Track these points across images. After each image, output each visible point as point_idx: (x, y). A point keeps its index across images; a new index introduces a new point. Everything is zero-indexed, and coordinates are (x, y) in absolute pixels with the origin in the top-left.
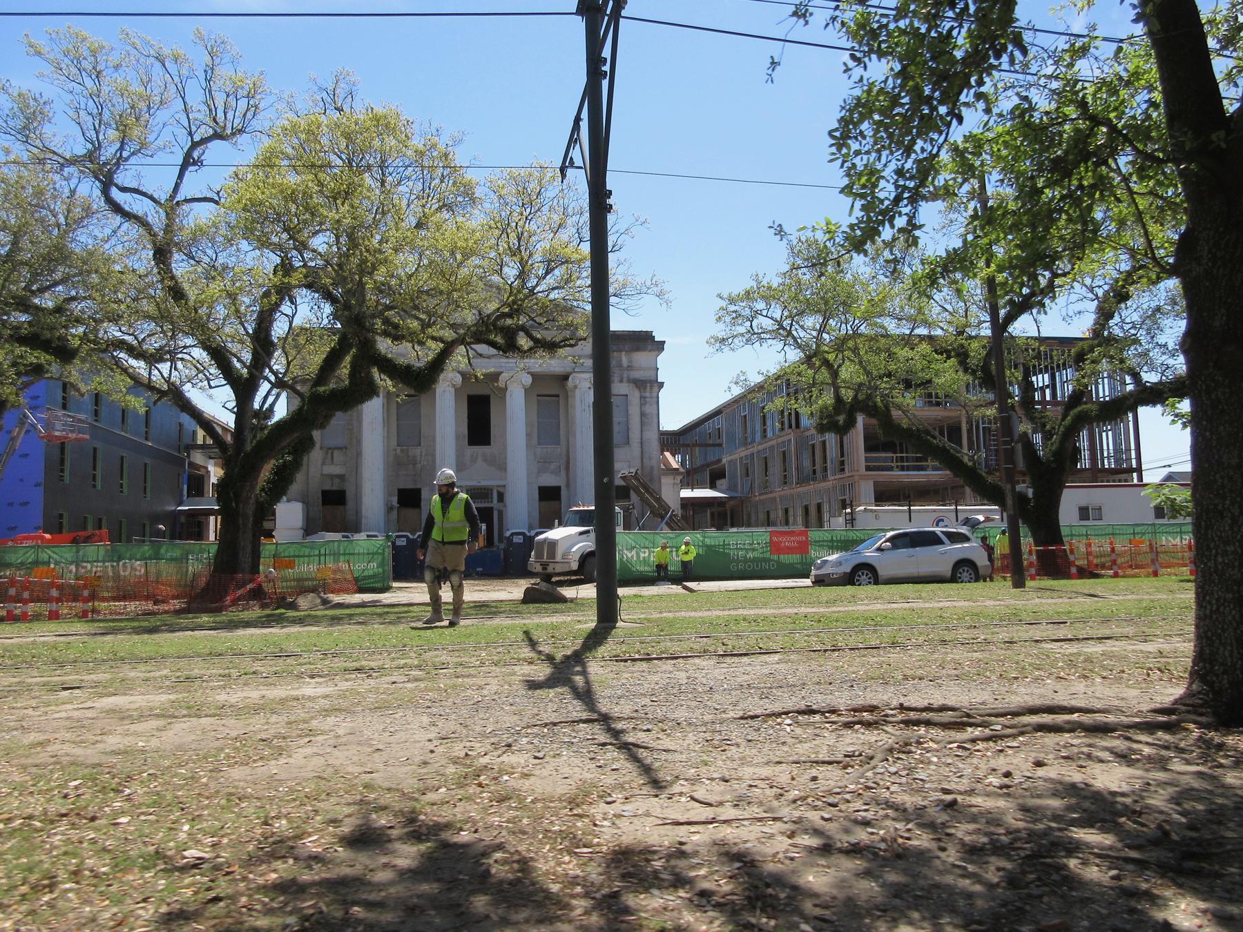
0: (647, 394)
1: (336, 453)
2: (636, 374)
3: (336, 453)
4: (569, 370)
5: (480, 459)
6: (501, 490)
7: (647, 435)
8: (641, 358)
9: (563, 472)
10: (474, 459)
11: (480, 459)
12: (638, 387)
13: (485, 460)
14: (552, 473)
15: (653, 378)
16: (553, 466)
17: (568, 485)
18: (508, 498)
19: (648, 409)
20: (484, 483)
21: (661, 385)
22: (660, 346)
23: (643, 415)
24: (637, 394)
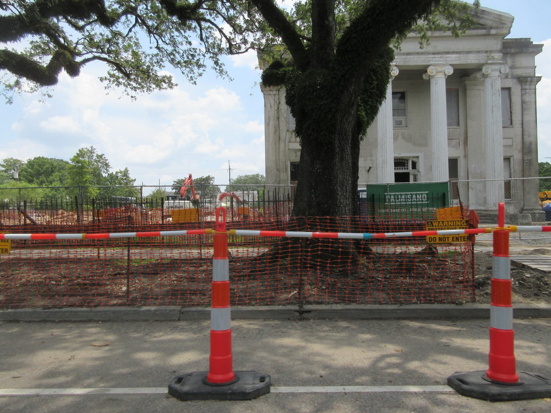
0: (527, 87)
2: (519, 72)
4: (482, 62)
5: (400, 137)
6: (415, 160)
7: (526, 118)
8: (522, 60)
9: (462, 147)
11: (400, 137)
13: (404, 138)
15: (532, 75)
16: (454, 142)
17: (466, 156)
18: (421, 166)
19: (527, 98)
20: (403, 155)
21: (539, 79)
22: (539, 48)
23: (523, 102)
24: (519, 87)
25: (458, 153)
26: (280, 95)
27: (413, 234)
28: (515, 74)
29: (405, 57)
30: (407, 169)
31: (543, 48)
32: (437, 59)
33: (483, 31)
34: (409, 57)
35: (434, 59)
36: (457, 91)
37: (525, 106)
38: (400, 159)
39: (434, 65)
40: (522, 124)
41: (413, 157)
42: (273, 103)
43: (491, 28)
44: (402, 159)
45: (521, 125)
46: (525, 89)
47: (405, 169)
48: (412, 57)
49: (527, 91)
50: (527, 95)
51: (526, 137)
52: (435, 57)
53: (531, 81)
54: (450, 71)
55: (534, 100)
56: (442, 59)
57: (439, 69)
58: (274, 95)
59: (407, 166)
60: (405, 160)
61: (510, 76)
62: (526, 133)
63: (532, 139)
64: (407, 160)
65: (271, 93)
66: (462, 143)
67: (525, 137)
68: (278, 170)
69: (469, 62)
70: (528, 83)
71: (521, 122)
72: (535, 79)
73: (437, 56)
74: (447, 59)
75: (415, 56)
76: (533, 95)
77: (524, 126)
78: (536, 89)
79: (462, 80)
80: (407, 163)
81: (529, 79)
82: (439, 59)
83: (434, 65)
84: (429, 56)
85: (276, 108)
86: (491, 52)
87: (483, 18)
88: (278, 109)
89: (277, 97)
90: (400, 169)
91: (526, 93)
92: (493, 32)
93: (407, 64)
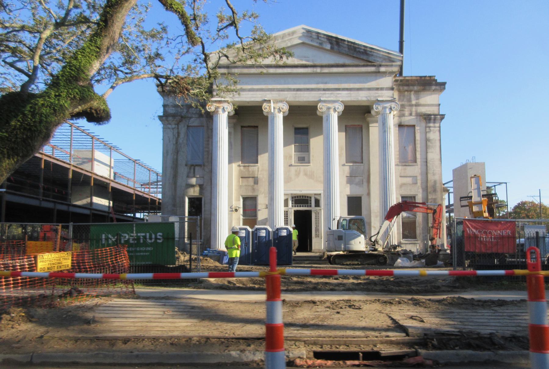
0: (431, 125)
1: (197, 168)
3: (197, 168)
6: (317, 197)
7: (430, 156)
9: (365, 184)
10: (298, 174)
12: (425, 119)
13: (306, 174)
14: (356, 184)
15: (436, 112)
16: (357, 180)
21: (442, 117)
22: (442, 86)
24: (423, 124)
25: (358, 192)
26: (180, 128)
27: (154, 277)
28: (419, 111)
29: (295, 92)
30: (310, 206)
31: (446, 86)
32: (327, 95)
33: (373, 69)
34: (299, 92)
35: (324, 96)
36: (361, 128)
37: (429, 143)
38: (303, 196)
39: (325, 101)
40: (427, 162)
41: (315, 194)
43: (380, 66)
44: (305, 197)
45: (425, 164)
46: (430, 127)
47: (308, 206)
48: (302, 93)
49: (432, 129)
50: (432, 132)
51: (430, 177)
52: (325, 94)
53: (435, 119)
54: (341, 108)
55: (438, 138)
56: (332, 95)
57: (329, 105)
58: (173, 129)
59: (311, 203)
60: (308, 197)
61: (414, 114)
62: (430, 172)
63: (437, 177)
64: (310, 198)
65: (170, 126)
66: (365, 180)
67: (429, 176)
68: (174, 205)
69: (360, 99)
70: (432, 121)
71: (425, 160)
72: (439, 117)
73: (327, 92)
74: (338, 96)
75: (306, 92)
76: (438, 133)
77: (428, 165)
78: (440, 127)
79: (357, 117)
80: (310, 201)
81: (432, 117)
82: (329, 95)
83: (325, 101)
84: (319, 92)
85: (175, 142)
86: (382, 89)
87: (372, 55)
88: (177, 143)
89: (176, 131)
90: (300, 206)
91: (429, 132)
92: (382, 69)
93: (297, 100)
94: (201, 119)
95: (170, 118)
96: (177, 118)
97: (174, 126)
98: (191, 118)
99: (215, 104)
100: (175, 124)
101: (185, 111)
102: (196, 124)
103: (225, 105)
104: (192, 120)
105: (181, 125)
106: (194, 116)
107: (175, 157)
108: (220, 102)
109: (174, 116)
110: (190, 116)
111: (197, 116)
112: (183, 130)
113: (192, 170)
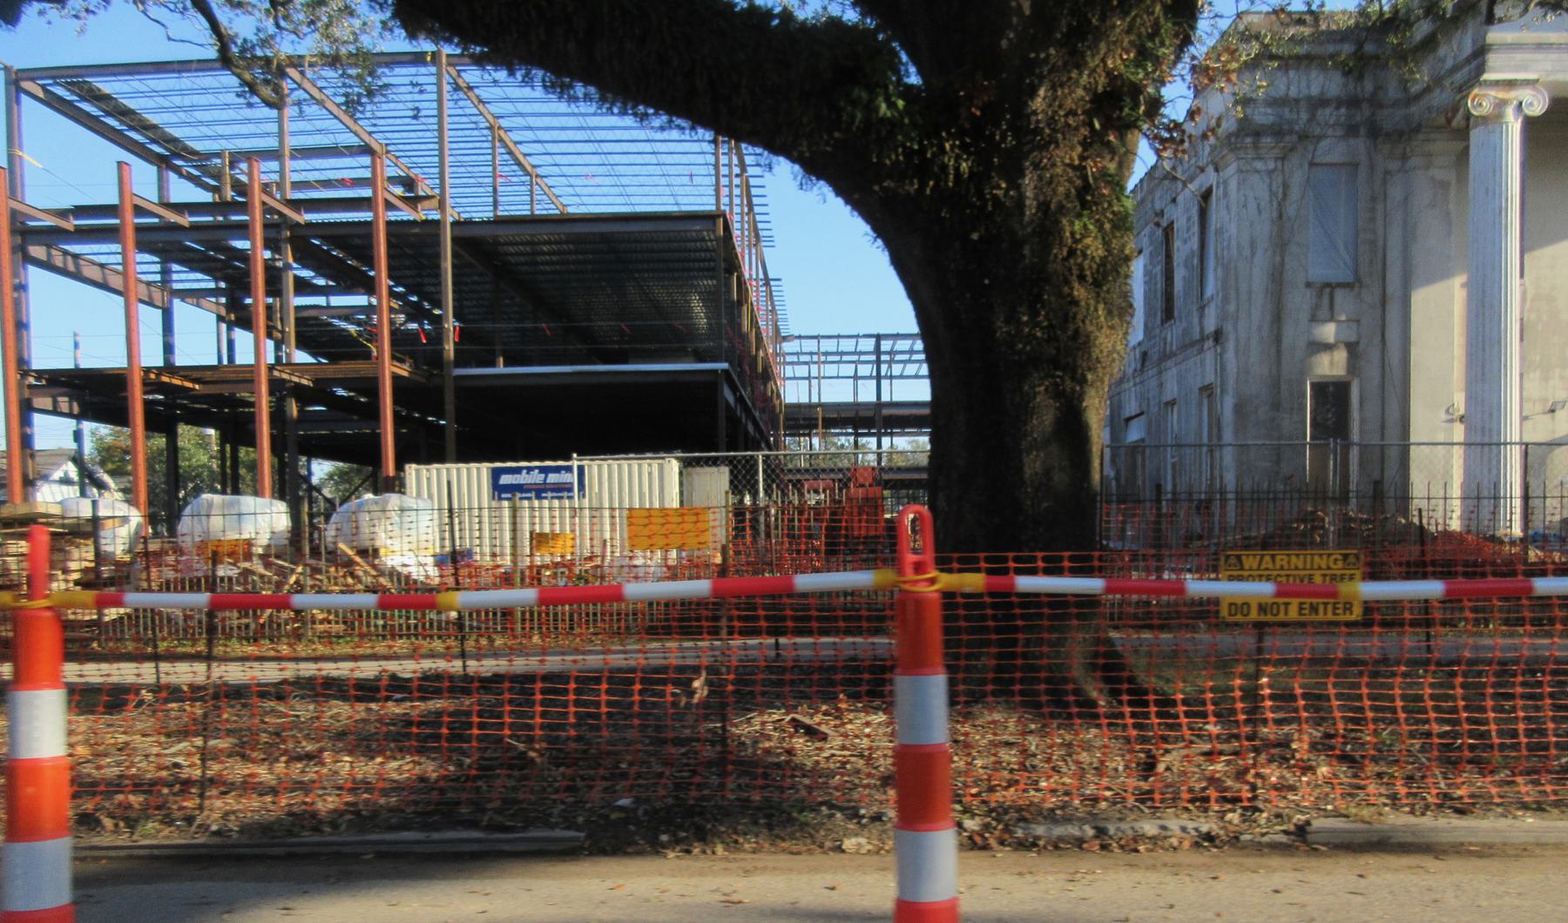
1: (1340, 295)
42: (1267, 197)
58: (1270, 173)
65: (1259, 165)
68: (1276, 406)
85: (1275, 215)
88: (1281, 216)
94: (1352, 141)
95: (1267, 141)
96: (1287, 138)
97: (1271, 165)
98: (1320, 138)
99: (1493, 93)
100: (1276, 159)
101: (1304, 116)
102: (1334, 157)
103: (1526, 95)
104: (1324, 143)
105: (1295, 159)
106: (1330, 132)
107: (1278, 259)
108: (1511, 84)
109: (1277, 131)
110: (1318, 131)
111: (1340, 132)
112: (1297, 178)
113: (1326, 301)
